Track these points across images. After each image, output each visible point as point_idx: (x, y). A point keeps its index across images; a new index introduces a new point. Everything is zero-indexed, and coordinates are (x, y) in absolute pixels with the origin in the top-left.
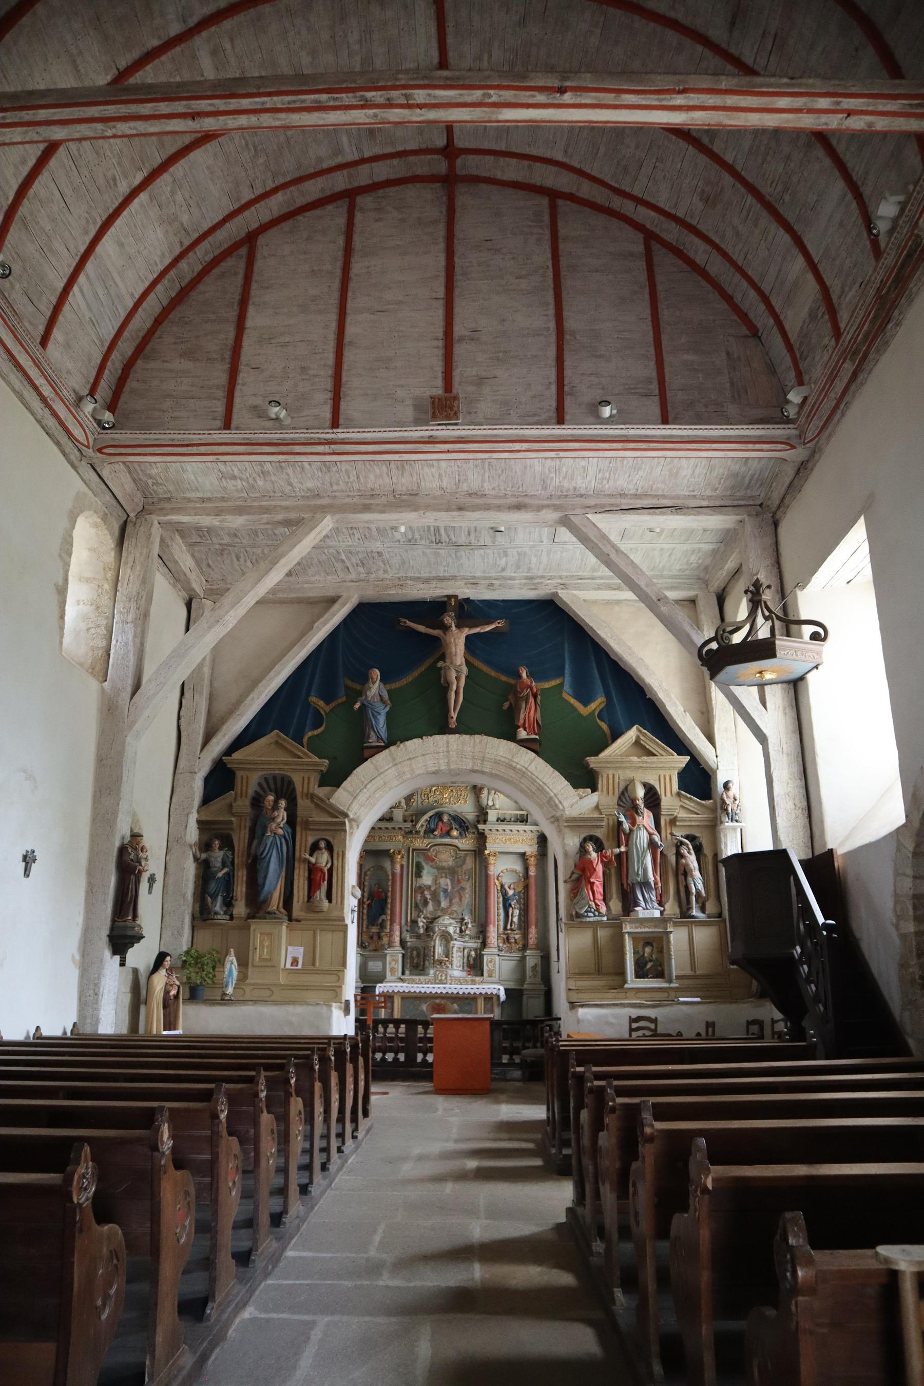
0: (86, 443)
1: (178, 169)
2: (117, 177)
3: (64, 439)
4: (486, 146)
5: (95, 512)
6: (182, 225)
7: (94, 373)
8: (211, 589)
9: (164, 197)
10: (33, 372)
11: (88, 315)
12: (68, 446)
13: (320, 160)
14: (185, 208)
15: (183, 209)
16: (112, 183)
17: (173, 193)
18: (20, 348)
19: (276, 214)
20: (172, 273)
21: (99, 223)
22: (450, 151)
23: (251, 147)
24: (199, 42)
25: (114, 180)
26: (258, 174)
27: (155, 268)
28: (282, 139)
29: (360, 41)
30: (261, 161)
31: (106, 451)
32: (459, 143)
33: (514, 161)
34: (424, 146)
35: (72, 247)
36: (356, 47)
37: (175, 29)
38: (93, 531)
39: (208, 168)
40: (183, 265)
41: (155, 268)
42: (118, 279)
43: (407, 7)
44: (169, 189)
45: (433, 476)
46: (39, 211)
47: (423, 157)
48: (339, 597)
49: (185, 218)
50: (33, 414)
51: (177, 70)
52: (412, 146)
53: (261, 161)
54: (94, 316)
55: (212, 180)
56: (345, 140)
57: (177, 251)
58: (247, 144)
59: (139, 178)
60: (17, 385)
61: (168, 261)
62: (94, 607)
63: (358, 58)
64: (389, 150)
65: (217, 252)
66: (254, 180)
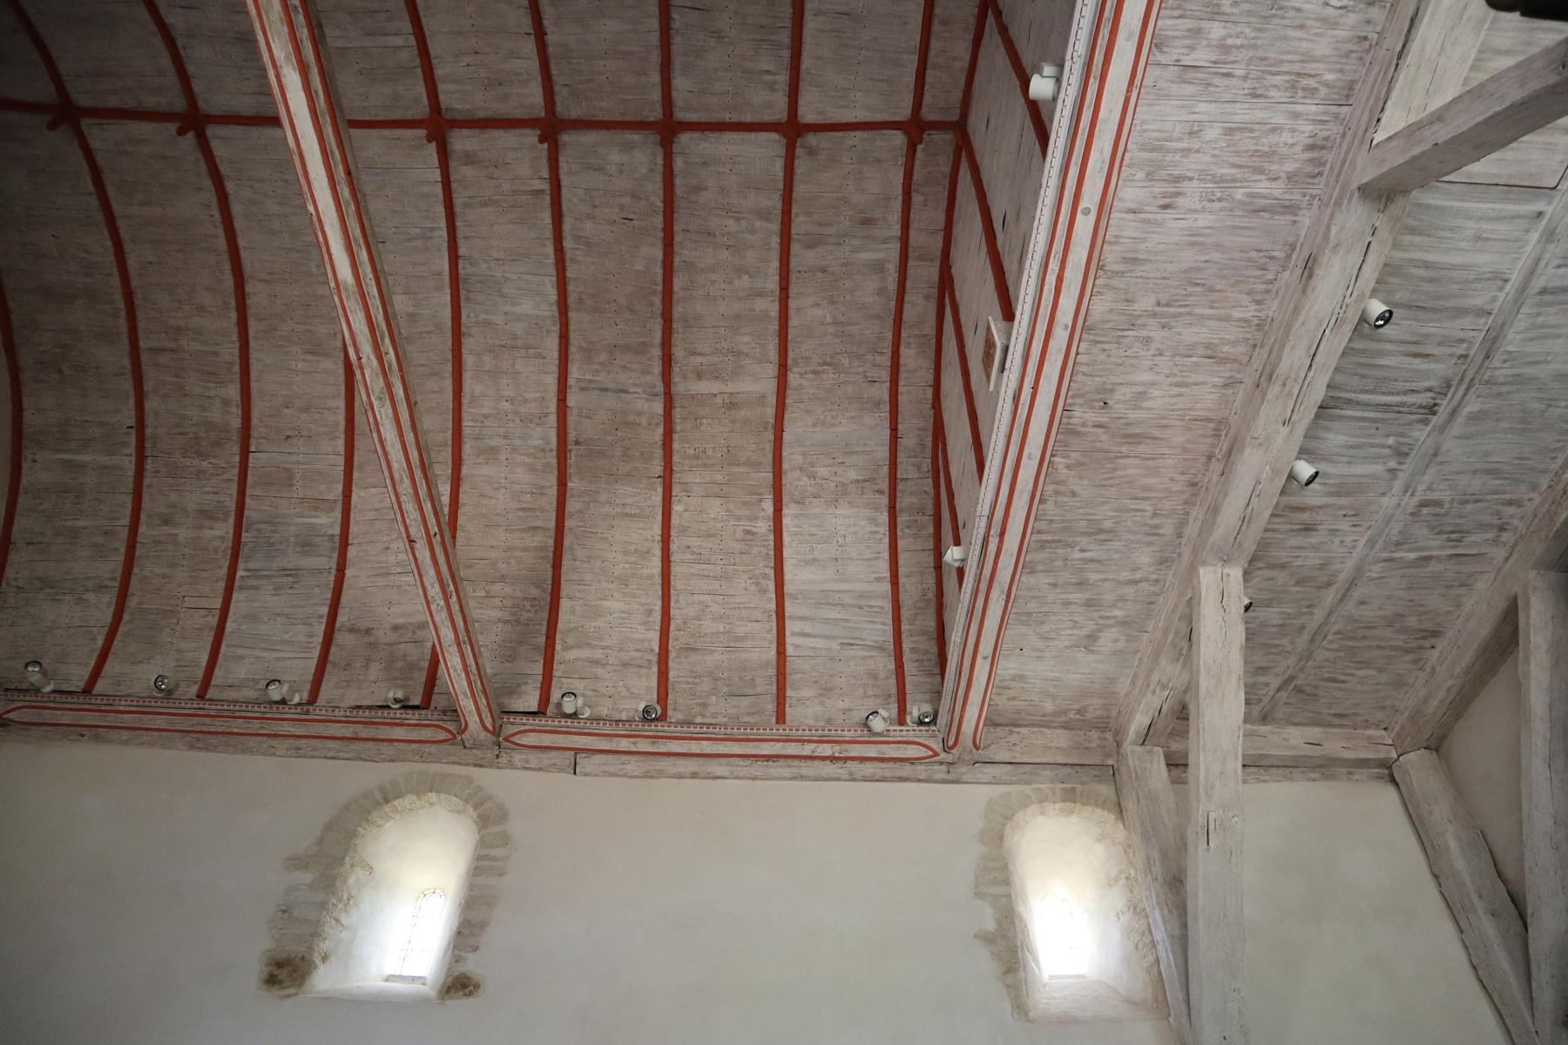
0: (931, 753)
1: (791, 457)
2: (748, 528)
3: (907, 770)
4: (909, 78)
5: (1040, 802)
6: (857, 481)
7: (893, 681)
8: (1398, 735)
9: (810, 489)
10: (792, 749)
11: (834, 645)
12: (920, 769)
13: (881, 291)
14: (839, 470)
15: (839, 472)
16: (750, 537)
17: (813, 476)
18: (751, 744)
19: (928, 364)
20: (902, 519)
21: (771, 573)
22: (915, 128)
23: (821, 369)
24: (680, 386)
25: (749, 532)
26: (860, 369)
27: (878, 536)
28: (831, 329)
29: (737, 219)
30: (846, 362)
31: (924, 752)
32: (903, 112)
33: (935, 44)
34: (902, 160)
35: (759, 615)
36: (744, 224)
37: (658, 407)
38: (1074, 819)
39: (815, 425)
40: (903, 501)
41: (878, 536)
42: (844, 586)
43: (705, 163)
44: (805, 479)
45: (1182, 395)
46: (700, 626)
47: (917, 163)
48: (1515, 600)
49: (853, 475)
50: (838, 779)
51: (696, 419)
52: (898, 177)
53: (846, 362)
54: (845, 638)
55: (833, 425)
56: (864, 256)
57: (885, 500)
58: (815, 372)
59: (768, 506)
60: (787, 772)
61: (884, 517)
62: (1132, 910)
63: (758, 224)
64: (897, 205)
65: (928, 452)
66: (866, 377)
